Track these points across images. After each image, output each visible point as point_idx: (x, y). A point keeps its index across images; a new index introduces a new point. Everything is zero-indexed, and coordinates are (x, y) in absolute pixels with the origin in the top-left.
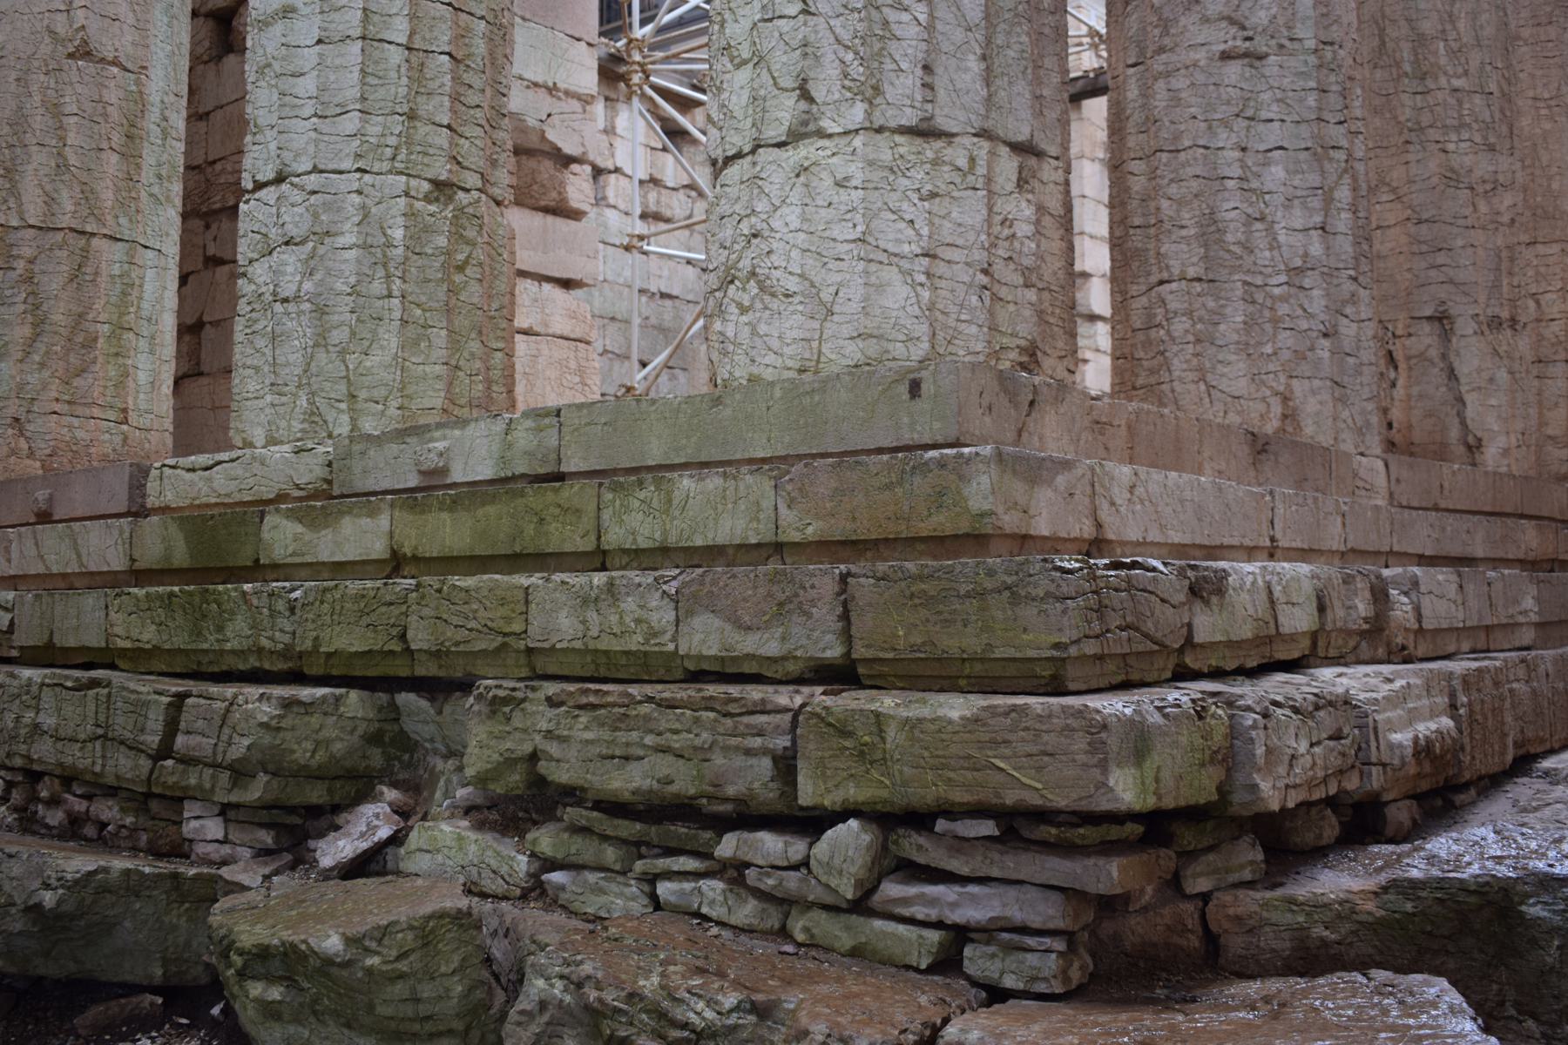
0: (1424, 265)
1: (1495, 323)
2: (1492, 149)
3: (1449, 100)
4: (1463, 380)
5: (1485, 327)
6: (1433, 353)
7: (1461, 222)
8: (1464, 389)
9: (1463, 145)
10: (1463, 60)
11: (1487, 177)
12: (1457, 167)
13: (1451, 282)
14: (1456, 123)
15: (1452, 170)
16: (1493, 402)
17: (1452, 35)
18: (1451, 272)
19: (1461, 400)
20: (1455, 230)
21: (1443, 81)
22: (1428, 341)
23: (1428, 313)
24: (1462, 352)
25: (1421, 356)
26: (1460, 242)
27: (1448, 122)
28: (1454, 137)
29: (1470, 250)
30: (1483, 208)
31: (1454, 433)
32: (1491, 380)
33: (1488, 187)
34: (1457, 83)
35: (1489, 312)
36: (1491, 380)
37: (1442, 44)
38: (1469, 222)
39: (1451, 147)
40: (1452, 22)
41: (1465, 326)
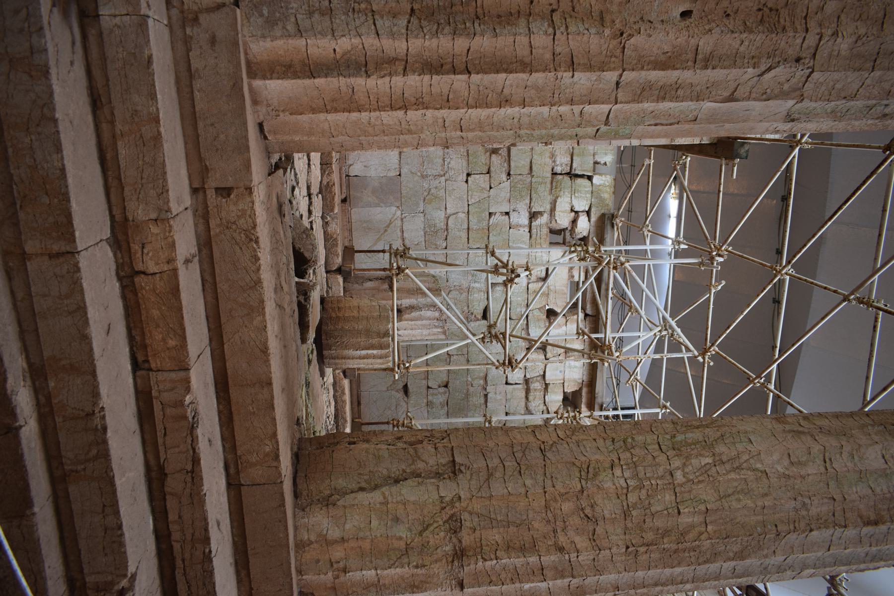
0: (503, 456)
1: (454, 525)
2: (626, 514)
3: (661, 469)
4: (394, 489)
5: (449, 511)
6: (421, 465)
7: (549, 483)
8: (384, 489)
9: (622, 481)
10: (701, 478)
11: (597, 509)
12: (601, 478)
13: (490, 475)
14: (641, 475)
15: (596, 475)
16: (375, 523)
17: (721, 469)
18: (498, 475)
19: (376, 487)
20: (540, 478)
21: (677, 463)
22: (432, 462)
23: (457, 460)
24: (423, 488)
25: (417, 457)
26: (528, 482)
27: (640, 468)
28: (627, 474)
29: (523, 490)
30: (567, 507)
31: (341, 483)
32: (397, 520)
33: (588, 511)
34: (679, 475)
35: (465, 516)
36: (397, 520)
37: (709, 460)
38: (549, 489)
39: (618, 472)
40: (734, 470)
41: (448, 490)
